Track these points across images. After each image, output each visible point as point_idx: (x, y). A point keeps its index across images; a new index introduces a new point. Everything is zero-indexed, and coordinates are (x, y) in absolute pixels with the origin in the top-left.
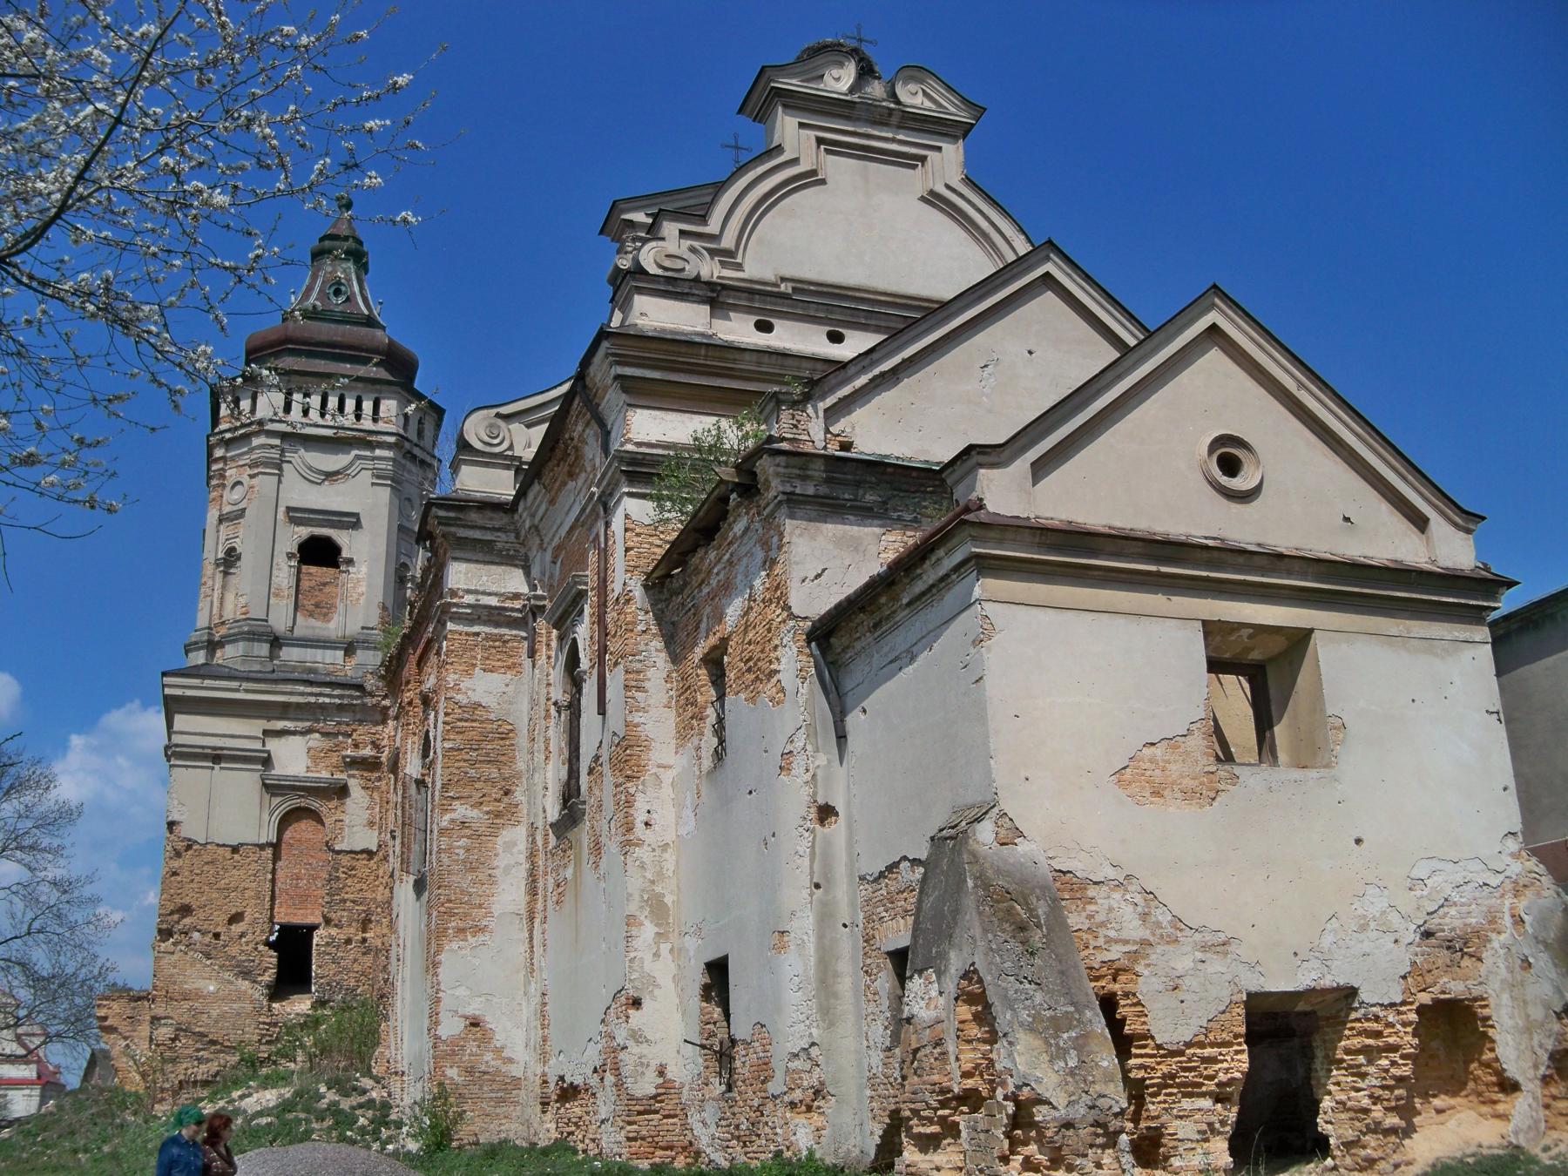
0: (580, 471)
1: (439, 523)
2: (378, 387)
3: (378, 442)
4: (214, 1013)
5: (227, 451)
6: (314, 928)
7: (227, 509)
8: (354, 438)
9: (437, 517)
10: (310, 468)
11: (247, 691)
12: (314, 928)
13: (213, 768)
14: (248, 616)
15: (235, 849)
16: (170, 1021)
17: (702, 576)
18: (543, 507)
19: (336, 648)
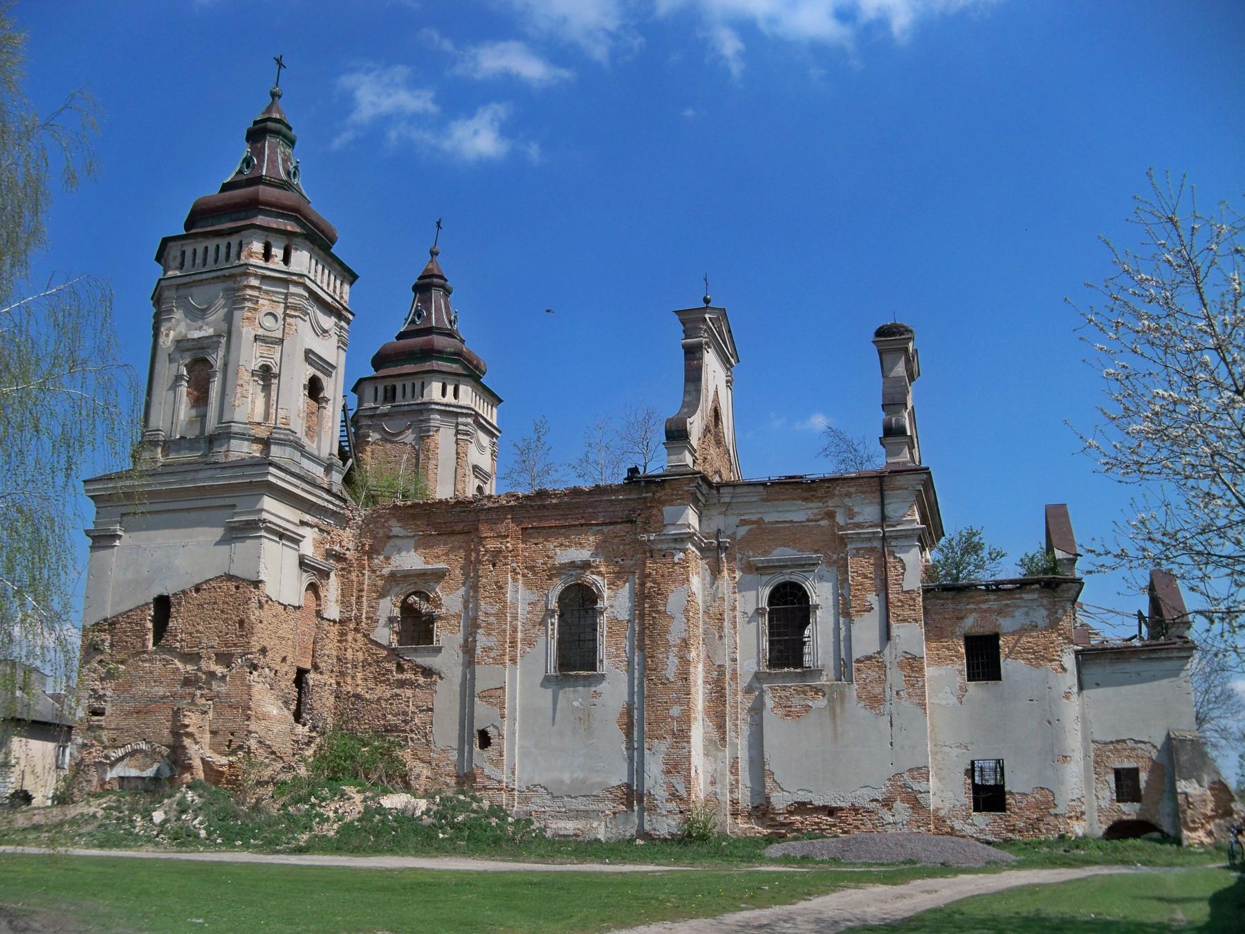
0: (820, 501)
1: (696, 487)
2: (345, 274)
3: (346, 317)
4: (275, 731)
5: (261, 283)
6: (307, 671)
7: (260, 332)
8: (337, 309)
9: (698, 483)
10: (318, 322)
11: (303, 490)
12: (307, 671)
13: (278, 542)
14: (287, 427)
15: (285, 607)
16: (256, 735)
17: (973, 600)
18: (755, 499)
19: (321, 465)
